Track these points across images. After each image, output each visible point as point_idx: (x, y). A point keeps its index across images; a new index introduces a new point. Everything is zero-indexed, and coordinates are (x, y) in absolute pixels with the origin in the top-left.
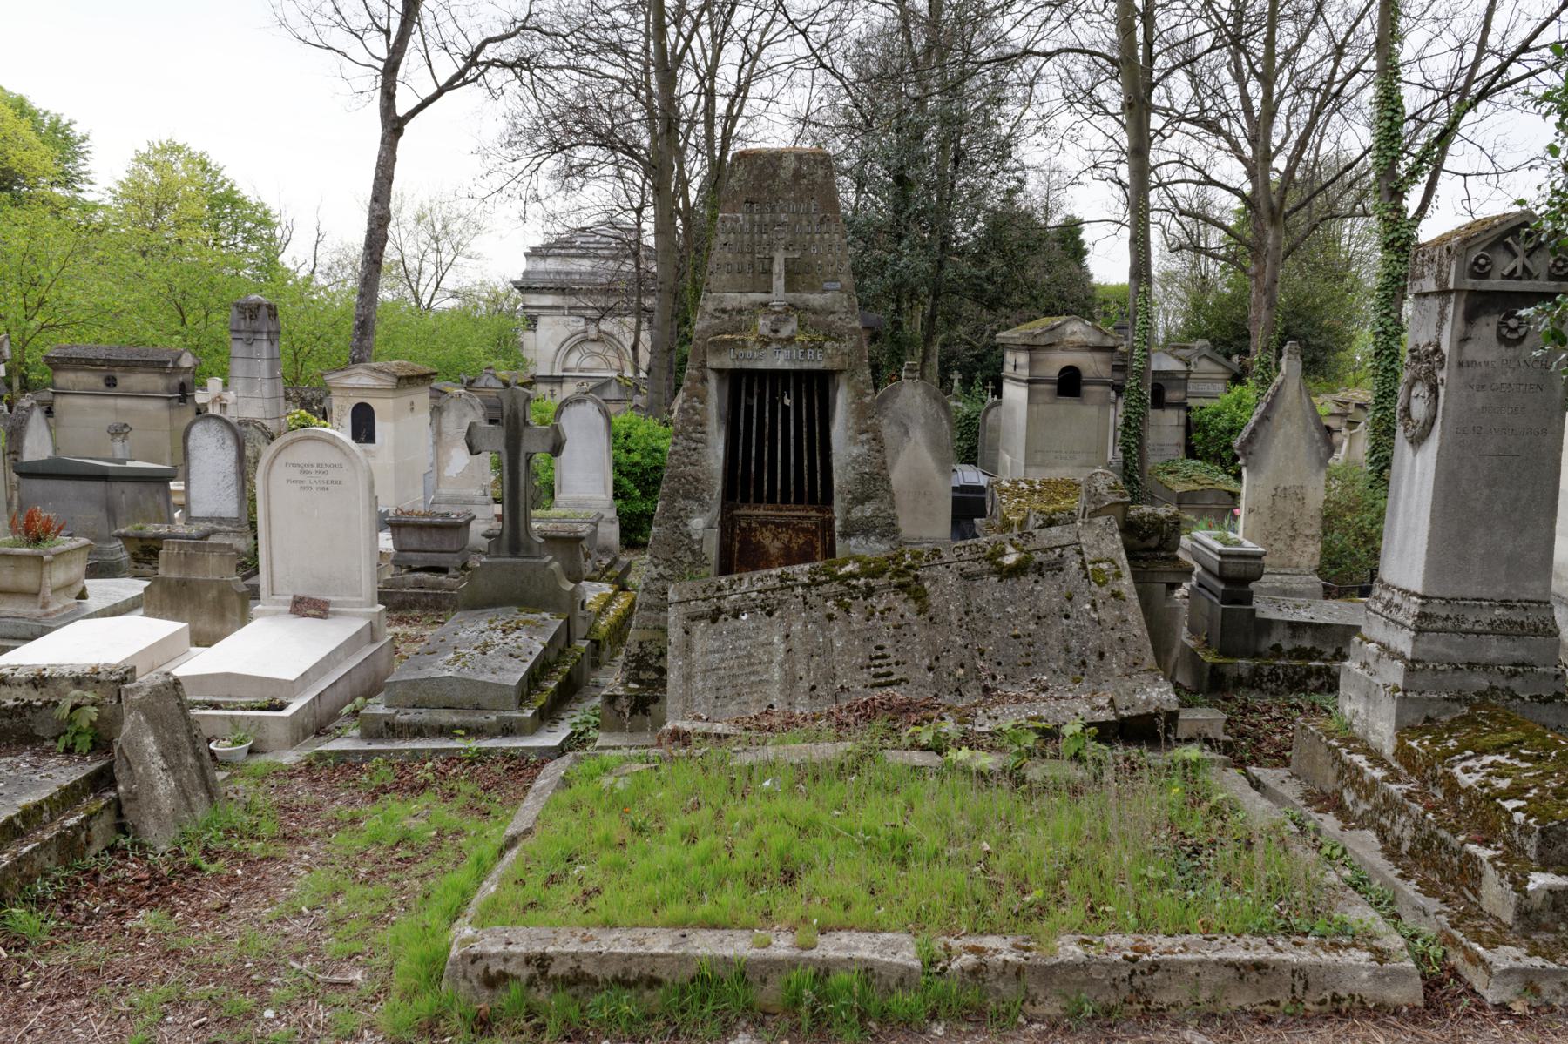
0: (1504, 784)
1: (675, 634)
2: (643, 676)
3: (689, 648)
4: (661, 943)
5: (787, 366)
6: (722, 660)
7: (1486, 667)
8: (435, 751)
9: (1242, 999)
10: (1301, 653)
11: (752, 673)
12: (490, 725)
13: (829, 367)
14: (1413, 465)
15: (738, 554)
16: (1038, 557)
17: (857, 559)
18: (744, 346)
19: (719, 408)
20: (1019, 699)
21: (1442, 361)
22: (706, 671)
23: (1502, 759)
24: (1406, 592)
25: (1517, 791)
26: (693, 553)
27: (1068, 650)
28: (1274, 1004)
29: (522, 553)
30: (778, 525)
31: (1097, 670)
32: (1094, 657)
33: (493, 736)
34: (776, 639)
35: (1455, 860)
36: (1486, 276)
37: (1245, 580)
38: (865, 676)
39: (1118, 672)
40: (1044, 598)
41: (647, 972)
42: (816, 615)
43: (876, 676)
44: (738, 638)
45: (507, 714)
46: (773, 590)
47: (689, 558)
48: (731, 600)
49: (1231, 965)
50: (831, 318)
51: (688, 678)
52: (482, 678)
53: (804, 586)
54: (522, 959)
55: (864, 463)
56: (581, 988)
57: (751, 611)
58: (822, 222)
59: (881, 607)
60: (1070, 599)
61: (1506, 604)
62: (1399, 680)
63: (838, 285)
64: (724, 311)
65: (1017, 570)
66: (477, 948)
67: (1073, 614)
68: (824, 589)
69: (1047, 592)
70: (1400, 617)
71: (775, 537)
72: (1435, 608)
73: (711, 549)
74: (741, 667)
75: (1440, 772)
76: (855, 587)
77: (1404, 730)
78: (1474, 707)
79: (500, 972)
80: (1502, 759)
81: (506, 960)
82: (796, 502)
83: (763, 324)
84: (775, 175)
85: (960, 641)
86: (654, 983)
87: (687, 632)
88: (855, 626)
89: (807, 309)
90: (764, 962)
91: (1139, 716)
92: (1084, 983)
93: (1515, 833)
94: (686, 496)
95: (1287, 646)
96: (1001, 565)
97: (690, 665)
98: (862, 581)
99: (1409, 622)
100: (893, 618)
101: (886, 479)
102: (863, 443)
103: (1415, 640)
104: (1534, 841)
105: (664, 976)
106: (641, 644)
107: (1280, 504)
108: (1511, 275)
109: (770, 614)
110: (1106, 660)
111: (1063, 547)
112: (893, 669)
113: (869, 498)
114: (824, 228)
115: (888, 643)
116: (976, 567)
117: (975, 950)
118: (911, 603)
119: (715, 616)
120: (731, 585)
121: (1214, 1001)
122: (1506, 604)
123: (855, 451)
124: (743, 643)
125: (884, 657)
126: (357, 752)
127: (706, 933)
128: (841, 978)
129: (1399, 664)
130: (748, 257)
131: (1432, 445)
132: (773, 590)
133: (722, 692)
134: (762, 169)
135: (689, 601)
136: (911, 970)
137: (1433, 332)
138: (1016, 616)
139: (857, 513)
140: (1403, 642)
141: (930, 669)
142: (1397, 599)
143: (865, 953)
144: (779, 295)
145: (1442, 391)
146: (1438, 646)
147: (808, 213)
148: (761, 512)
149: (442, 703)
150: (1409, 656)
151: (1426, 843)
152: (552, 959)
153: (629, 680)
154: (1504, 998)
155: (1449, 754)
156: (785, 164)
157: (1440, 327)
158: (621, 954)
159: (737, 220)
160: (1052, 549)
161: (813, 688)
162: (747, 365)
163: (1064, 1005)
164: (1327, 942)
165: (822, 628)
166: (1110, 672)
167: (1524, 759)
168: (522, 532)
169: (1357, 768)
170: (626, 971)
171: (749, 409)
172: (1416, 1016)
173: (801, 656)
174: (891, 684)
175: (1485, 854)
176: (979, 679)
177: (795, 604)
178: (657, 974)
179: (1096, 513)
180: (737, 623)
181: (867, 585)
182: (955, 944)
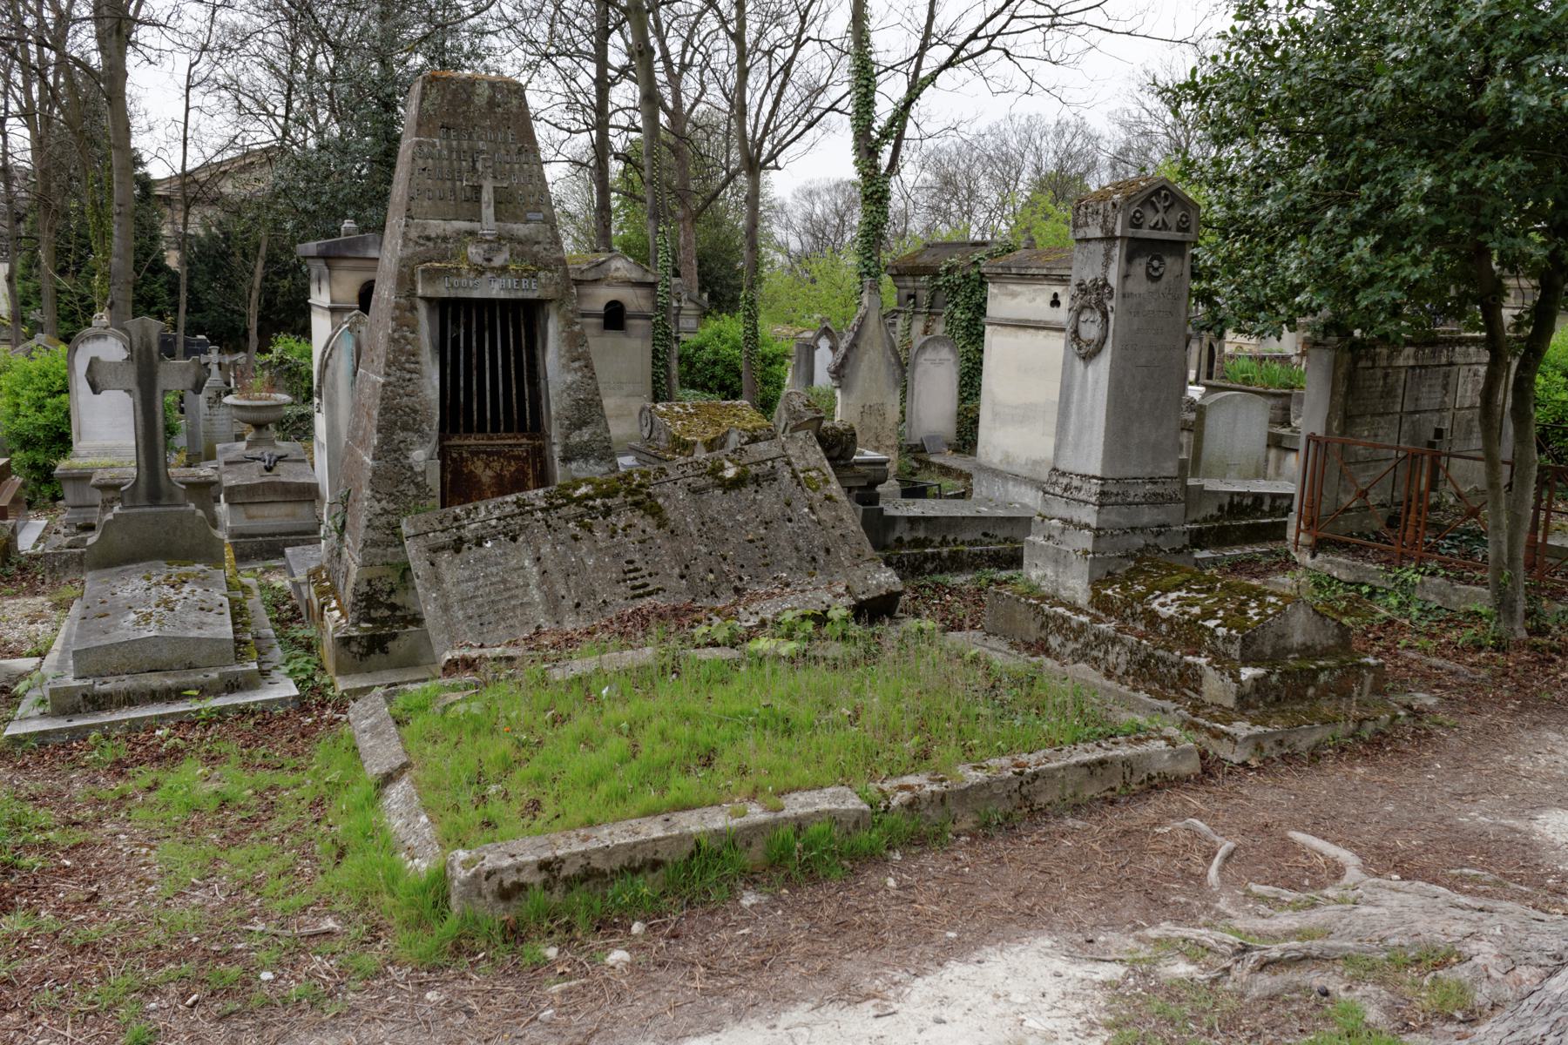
0: (1196, 610)
1: (419, 566)
2: (374, 614)
3: (438, 580)
4: (655, 829)
5: (503, 295)
6: (477, 588)
7: (1142, 529)
8: (162, 717)
9: (1093, 790)
10: (918, 543)
11: (512, 597)
12: (212, 683)
13: (543, 296)
14: (1085, 376)
15: (459, 487)
16: (753, 470)
17: (588, 482)
18: (459, 275)
19: (432, 338)
20: (770, 595)
21: (1111, 292)
22: (462, 600)
23: (1183, 594)
24: (1083, 476)
25: (1211, 615)
26: (417, 485)
27: (797, 549)
28: (1113, 789)
29: (163, 502)
30: (489, 454)
31: (827, 564)
32: (822, 553)
33: (217, 694)
34: (527, 563)
35: (1174, 671)
36: (1139, 226)
37: (873, 485)
38: (622, 588)
39: (847, 563)
40: (766, 505)
41: (650, 856)
42: (562, 536)
43: (634, 588)
44: (487, 565)
45: (230, 669)
46: (512, 516)
47: (413, 491)
48: (471, 529)
49: (1084, 765)
50: (536, 248)
51: (446, 608)
52: (191, 634)
53: (542, 510)
54: (535, 867)
55: (578, 390)
56: (591, 883)
57: (494, 538)
58: (520, 152)
59: (622, 525)
60: (788, 505)
61: (1152, 481)
62: (1089, 546)
63: (541, 216)
64: (428, 239)
65: (738, 483)
66: (488, 865)
67: (795, 517)
68: (564, 511)
69: (768, 500)
70: (1082, 496)
71: (487, 465)
72: (1112, 488)
73: (434, 480)
74: (498, 593)
75: (1139, 609)
76: (593, 508)
77: (1096, 584)
78: (1138, 561)
79: (514, 883)
80: (1183, 594)
81: (519, 870)
82: (506, 431)
83: (474, 252)
84: (469, 101)
85: (704, 550)
86: (656, 865)
87: (432, 564)
88: (602, 545)
89: (512, 239)
90: (749, 828)
91: (874, 599)
92: (988, 799)
93: (1219, 643)
94: (405, 428)
95: (907, 538)
96: (722, 478)
97: (445, 595)
98: (598, 501)
99: (1093, 499)
100: (635, 534)
101: (599, 404)
102: (575, 370)
103: (1099, 513)
104: (1237, 646)
105: (664, 857)
106: (369, 582)
107: (866, 420)
108: (1154, 228)
109: (514, 539)
110: (833, 555)
111: (773, 460)
112: (648, 580)
113: (586, 424)
114: (523, 159)
115: (637, 557)
116: (701, 482)
117: (902, 788)
118: (649, 519)
119: (458, 546)
120: (468, 514)
121: (1075, 795)
122: (1152, 481)
123: (569, 378)
124: (494, 570)
125: (636, 570)
126: (59, 731)
127: (687, 814)
128: (814, 829)
129: (1087, 532)
130: (449, 184)
131: (1104, 362)
132: (512, 516)
133: (485, 619)
134: (455, 93)
135: (426, 533)
136: (863, 812)
137: (1099, 271)
138: (746, 523)
139: (575, 438)
140: (1088, 515)
141: (682, 577)
142: (1076, 482)
143: (824, 806)
144: (488, 223)
145: (1112, 317)
146: (1114, 516)
147: (505, 142)
148: (472, 442)
149: (147, 667)
150: (1094, 525)
151: (1144, 664)
152: (563, 861)
153: (359, 620)
154: (1244, 758)
155: (1141, 597)
156: (479, 91)
157: (1106, 266)
158: (626, 845)
159: (434, 145)
160: (764, 462)
161: (578, 605)
162: (462, 294)
163: (976, 818)
164: (1132, 737)
165: (570, 548)
166: (840, 564)
167: (1198, 592)
168: (163, 479)
169: (1062, 616)
170: (632, 859)
171: (456, 341)
172: (1200, 781)
173: (557, 576)
174: (650, 594)
175: (1202, 661)
176: (728, 581)
177: (539, 529)
178: (659, 856)
179: (795, 429)
180: (483, 552)
181: (604, 505)
182: (886, 786)
